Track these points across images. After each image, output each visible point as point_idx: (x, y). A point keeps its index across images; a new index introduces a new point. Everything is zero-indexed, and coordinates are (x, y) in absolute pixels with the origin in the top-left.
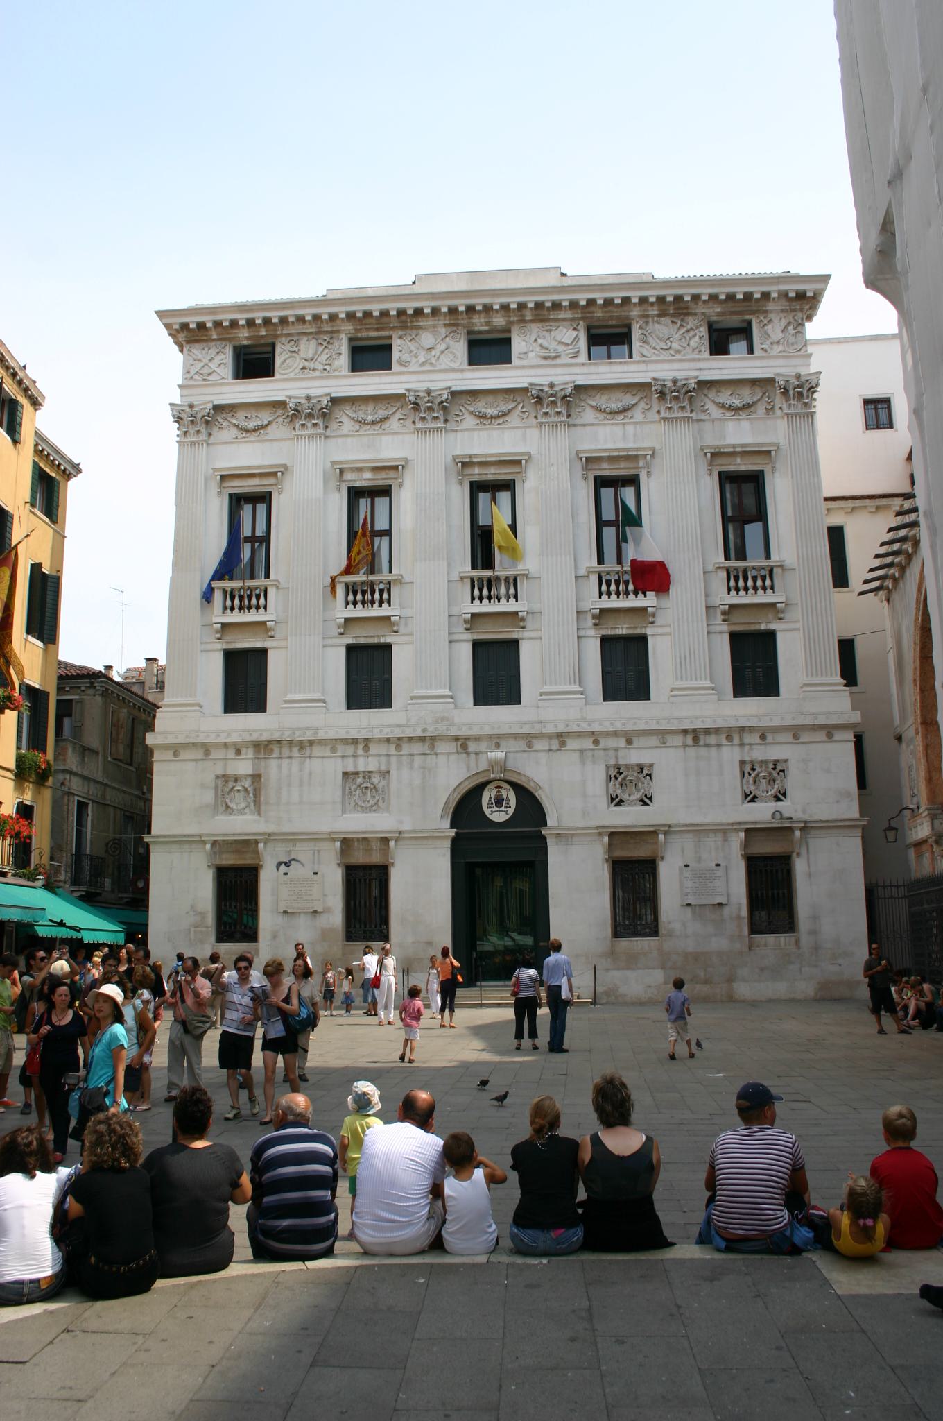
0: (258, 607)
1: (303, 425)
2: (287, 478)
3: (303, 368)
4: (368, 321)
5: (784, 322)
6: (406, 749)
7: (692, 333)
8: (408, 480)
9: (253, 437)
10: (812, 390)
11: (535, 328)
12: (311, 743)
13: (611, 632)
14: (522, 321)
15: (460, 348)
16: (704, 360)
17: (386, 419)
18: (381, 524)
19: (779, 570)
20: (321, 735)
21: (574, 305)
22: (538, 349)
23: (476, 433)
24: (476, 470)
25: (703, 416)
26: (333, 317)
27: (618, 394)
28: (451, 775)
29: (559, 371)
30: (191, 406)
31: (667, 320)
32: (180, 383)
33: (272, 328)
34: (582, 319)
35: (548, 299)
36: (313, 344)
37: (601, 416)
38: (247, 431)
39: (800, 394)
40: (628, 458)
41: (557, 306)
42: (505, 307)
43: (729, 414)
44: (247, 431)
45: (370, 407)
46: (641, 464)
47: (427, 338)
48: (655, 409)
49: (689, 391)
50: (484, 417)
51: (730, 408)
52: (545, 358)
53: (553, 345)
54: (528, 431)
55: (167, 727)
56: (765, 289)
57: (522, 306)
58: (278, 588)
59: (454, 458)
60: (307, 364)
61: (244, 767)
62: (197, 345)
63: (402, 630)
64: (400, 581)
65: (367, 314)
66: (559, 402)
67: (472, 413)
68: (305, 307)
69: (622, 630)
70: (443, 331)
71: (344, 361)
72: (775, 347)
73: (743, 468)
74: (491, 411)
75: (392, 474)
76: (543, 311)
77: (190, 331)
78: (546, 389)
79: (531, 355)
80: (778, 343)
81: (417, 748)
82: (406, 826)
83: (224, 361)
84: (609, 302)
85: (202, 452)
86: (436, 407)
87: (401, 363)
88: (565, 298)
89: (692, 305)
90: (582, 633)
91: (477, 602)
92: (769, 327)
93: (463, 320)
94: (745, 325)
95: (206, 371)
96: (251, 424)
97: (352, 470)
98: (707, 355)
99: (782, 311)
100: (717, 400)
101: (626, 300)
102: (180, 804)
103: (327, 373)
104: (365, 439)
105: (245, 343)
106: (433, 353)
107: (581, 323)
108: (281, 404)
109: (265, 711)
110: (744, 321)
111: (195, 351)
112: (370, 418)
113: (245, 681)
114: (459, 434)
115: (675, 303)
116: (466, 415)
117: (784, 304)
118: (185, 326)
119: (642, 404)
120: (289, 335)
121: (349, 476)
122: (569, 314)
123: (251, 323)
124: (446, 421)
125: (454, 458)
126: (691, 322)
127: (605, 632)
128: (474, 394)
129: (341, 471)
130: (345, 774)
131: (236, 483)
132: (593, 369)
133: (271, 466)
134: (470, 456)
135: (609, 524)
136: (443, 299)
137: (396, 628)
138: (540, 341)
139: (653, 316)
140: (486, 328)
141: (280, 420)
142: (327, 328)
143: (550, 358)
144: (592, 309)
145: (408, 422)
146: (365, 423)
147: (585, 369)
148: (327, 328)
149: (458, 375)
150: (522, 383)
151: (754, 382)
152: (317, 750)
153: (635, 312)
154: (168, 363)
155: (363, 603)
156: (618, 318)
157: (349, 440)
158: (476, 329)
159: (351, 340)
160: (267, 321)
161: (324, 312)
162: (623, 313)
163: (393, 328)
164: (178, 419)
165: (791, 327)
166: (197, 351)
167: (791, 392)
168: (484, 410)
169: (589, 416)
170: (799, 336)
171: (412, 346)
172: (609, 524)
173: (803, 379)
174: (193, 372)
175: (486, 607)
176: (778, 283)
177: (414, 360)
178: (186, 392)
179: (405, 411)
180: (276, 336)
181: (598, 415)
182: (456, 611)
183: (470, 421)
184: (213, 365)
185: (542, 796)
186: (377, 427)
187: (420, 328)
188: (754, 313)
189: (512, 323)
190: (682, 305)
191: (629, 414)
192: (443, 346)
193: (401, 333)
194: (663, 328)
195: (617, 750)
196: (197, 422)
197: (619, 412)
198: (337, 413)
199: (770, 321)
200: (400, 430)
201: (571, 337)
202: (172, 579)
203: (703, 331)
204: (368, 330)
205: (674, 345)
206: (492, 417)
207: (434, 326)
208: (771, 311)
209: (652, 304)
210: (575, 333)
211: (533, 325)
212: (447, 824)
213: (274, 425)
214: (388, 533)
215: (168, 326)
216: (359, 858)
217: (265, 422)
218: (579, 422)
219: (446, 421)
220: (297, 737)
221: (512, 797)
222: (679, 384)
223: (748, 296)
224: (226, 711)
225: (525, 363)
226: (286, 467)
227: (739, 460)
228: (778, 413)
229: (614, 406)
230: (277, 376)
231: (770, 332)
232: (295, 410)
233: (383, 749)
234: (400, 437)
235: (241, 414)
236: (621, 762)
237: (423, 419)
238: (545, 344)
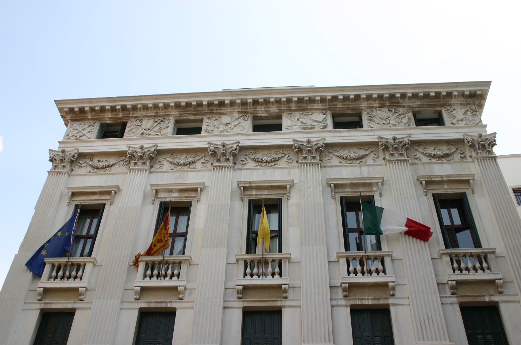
0: (76, 277)
1: (136, 163)
2: (118, 195)
3: (142, 134)
5: (463, 110)
7: (402, 116)
8: (204, 198)
10: (493, 144)
11: (297, 115)
13: (358, 302)
14: (290, 111)
15: (248, 124)
16: (413, 129)
17: (193, 162)
18: (181, 229)
19: (492, 255)
21: (323, 100)
22: (300, 124)
23: (255, 171)
24: (254, 192)
25: (416, 161)
26: (166, 106)
27: (355, 150)
29: (314, 135)
31: (386, 109)
32: (61, 139)
33: (126, 112)
34: (329, 109)
36: (151, 122)
37: (344, 162)
38: (97, 168)
39: (483, 146)
40: (364, 185)
41: (312, 101)
42: (278, 102)
43: (434, 160)
44: (97, 168)
45: (184, 156)
46: (374, 189)
47: (225, 119)
48: (382, 157)
49: (405, 145)
51: (434, 157)
52: (304, 129)
53: (310, 123)
54: (292, 170)
56: (449, 90)
57: (289, 101)
58: (95, 265)
59: (239, 183)
60: (145, 131)
62: (77, 123)
63: (186, 298)
64: (189, 262)
65: (188, 105)
66: (314, 152)
67: (253, 160)
68: (149, 99)
69: (368, 301)
70: (237, 116)
72: (460, 123)
73: (450, 191)
74: (265, 158)
75: (193, 194)
76: (302, 102)
77: (74, 113)
78: (304, 144)
79: (294, 127)
80: (462, 120)
84: (346, 98)
85: (64, 178)
86: (228, 154)
87: (207, 131)
89: (401, 101)
90: (334, 303)
91: (248, 277)
92: (454, 112)
93: (250, 109)
94: (436, 116)
95: (80, 134)
96: (101, 164)
98: (414, 126)
99: (461, 104)
100: (425, 152)
101: (358, 97)
104: (177, 174)
105: (109, 122)
106: (229, 126)
107: (328, 111)
110: (436, 112)
111: (75, 125)
112: (182, 162)
114: (243, 172)
115: (391, 99)
117: (462, 100)
118: (72, 110)
119: (372, 155)
120: (137, 117)
121: (161, 195)
122: (320, 106)
123: (113, 109)
124: (235, 164)
125: (239, 183)
126: (401, 110)
127: (353, 302)
128: (255, 149)
129: (157, 192)
132: (337, 134)
133: (108, 187)
134: (250, 183)
135: (352, 230)
136: (238, 95)
137: (181, 296)
138: (300, 120)
139: (375, 107)
140: (266, 115)
141: (122, 163)
142: (162, 113)
143: (306, 129)
144: (335, 103)
146: (178, 164)
147: (332, 134)
148: (162, 113)
149: (246, 138)
150: (290, 142)
151: (449, 142)
153: (364, 105)
154: (55, 132)
155: (158, 276)
156: (353, 108)
157: (166, 174)
158: (259, 115)
159: (177, 122)
160: (124, 108)
162: (356, 105)
164: (52, 160)
165: (469, 113)
166: (76, 125)
167: (477, 146)
168: (261, 157)
169: (335, 161)
170: (475, 117)
171: (216, 123)
172: (352, 230)
173: (483, 138)
174: (70, 135)
175: (256, 281)
176: (457, 87)
177: (216, 130)
178: (62, 146)
179: (207, 158)
180: (129, 118)
181: (342, 161)
182: (231, 284)
183: (251, 164)
184: (84, 132)
187: (222, 114)
188: (443, 106)
189: (282, 111)
190: (394, 101)
191: (364, 160)
192: (236, 122)
193: (209, 116)
194: (384, 113)
197: (356, 159)
198: (160, 159)
199: (454, 109)
200: (203, 169)
201: (321, 118)
202: (16, 256)
203: (410, 115)
205: (391, 122)
206: (267, 162)
208: (454, 105)
209: (375, 99)
210: (324, 116)
211: (296, 113)
213: (117, 166)
214: (184, 235)
215: (60, 110)
217: (111, 163)
218: (328, 164)
219: (235, 164)
222: (397, 141)
223: (438, 95)
225: (291, 131)
226: (118, 187)
227: (446, 187)
228: (470, 159)
229: (352, 155)
230: (125, 137)
231: (455, 115)
232: (131, 154)
234: (202, 173)
238: (304, 121)
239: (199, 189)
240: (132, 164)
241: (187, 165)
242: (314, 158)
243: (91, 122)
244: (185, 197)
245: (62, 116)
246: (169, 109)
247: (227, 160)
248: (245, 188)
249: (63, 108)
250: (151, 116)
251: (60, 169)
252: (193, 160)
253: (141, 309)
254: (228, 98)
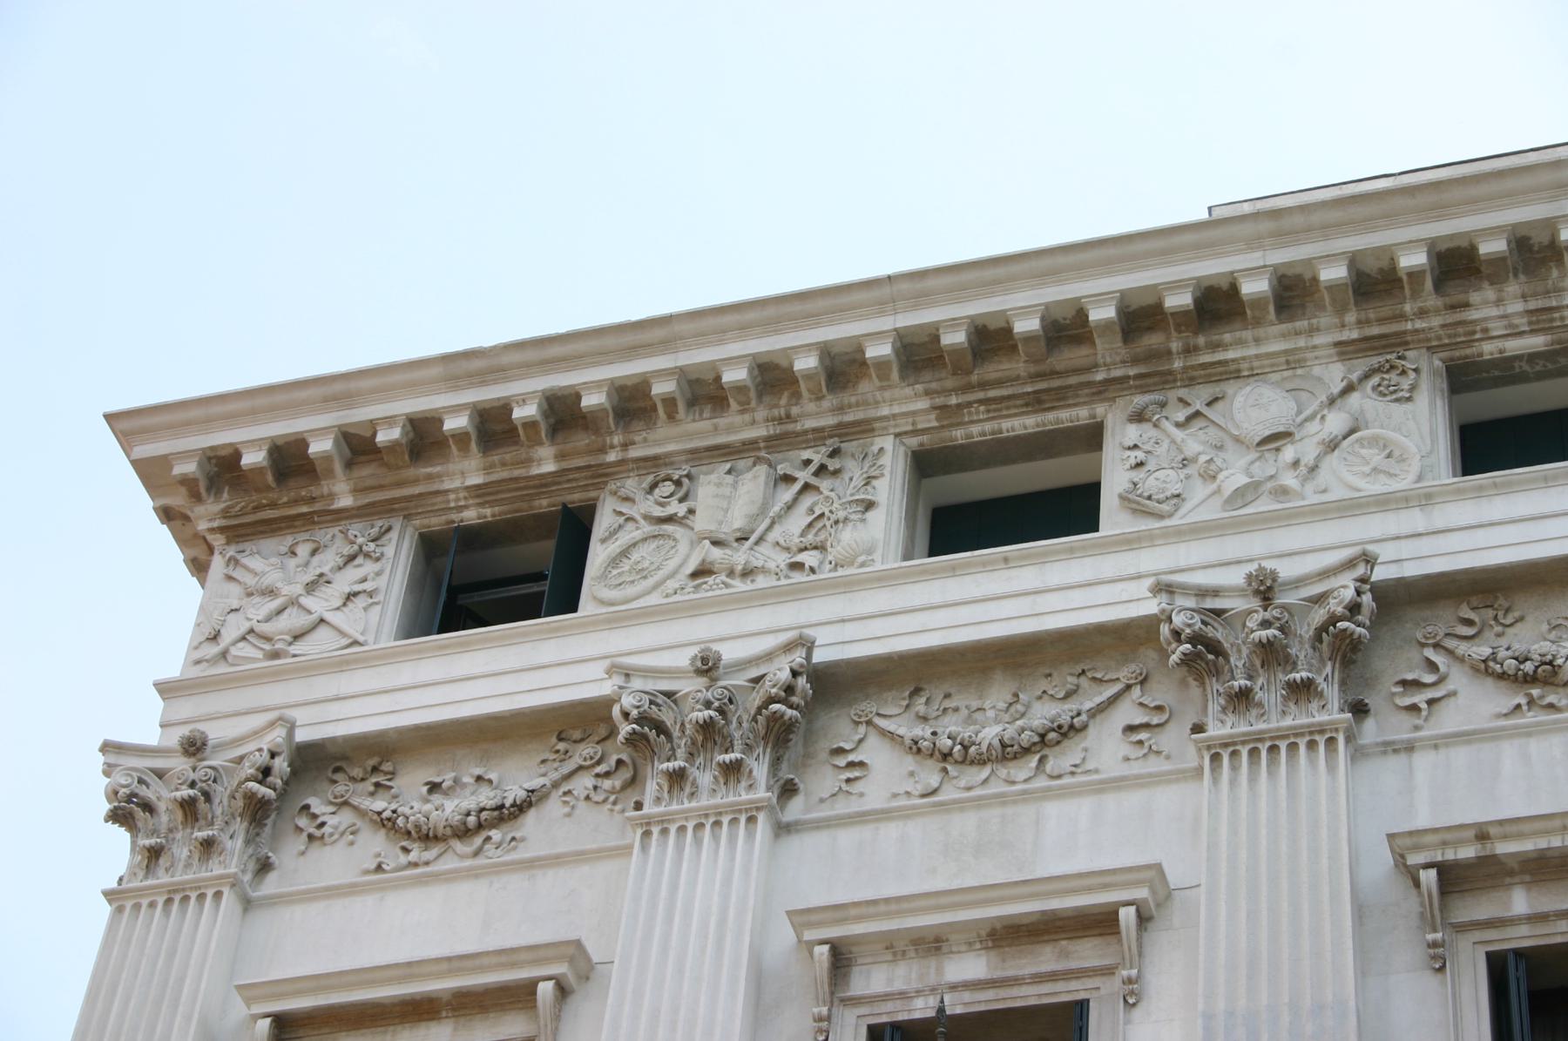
2: (581, 1008)
3: (701, 572)
4: (993, 369)
9: (456, 857)
15: (1420, 425)
17: (1068, 731)
23: (1509, 751)
24: (1520, 902)
26: (842, 368)
32: (173, 669)
33: (582, 440)
36: (753, 483)
38: (428, 837)
44: (428, 837)
45: (997, 696)
47: (1255, 407)
60: (717, 553)
62: (271, 544)
65: (991, 339)
67: (1486, 669)
70: (1335, 374)
75: (1088, 953)
77: (240, 487)
85: (214, 924)
86: (1299, 650)
87: (1136, 504)
93: (1424, 314)
95: (292, 620)
96: (450, 809)
97: (897, 947)
104: (965, 824)
105: (471, 516)
106: (1289, 453)
111: (255, 563)
112: (990, 734)
114: (1423, 761)
116: (1458, 679)
118: (223, 469)
120: (654, 461)
121: (872, 979)
123: (494, 428)
124: (1360, 710)
129: (841, 959)
133: (508, 956)
134: (1482, 834)
136: (1327, 230)
140: (1537, 342)
141: (584, 782)
142: (815, 415)
146: (963, 755)
148: (815, 415)
149: (1414, 520)
154: (131, 619)
158: (1489, 349)
159: (925, 464)
160: (563, 414)
161: (801, 348)
163: (1106, 390)
164: (127, 811)
166: (264, 562)
171: (1193, 442)
174: (228, 635)
177: (1200, 491)
178: (186, 708)
179: (1161, 692)
180: (601, 475)
183: (1473, 703)
184: (317, 605)
186: (1023, 770)
187: (1231, 373)
192: (1336, 422)
193: (1140, 400)
198: (840, 729)
200: (1136, 768)
204: (996, 406)
207: (1292, 361)
215: (151, 473)
219: (1360, 710)
226: (575, 951)
230: (586, 606)
232: (642, 719)
234: (1133, 799)
235: (410, 784)
237: (1241, 699)
239: (1127, 916)
240: (652, 787)
241: (1027, 751)
243: (355, 529)
244: (1039, 978)
245: (167, 515)
246: (866, 387)
247: (1302, 691)
248: (1453, 879)
249: (165, 461)
250: (749, 447)
251: (181, 867)
252: (1062, 712)
254: (1254, 259)
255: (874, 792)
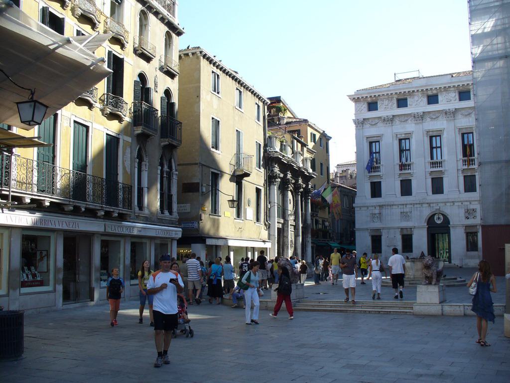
6: (416, 206)
8: (414, 136)
9: (374, 126)
12: (393, 205)
14: (441, 91)
15: (425, 100)
20: (395, 203)
21: (454, 86)
28: (427, 212)
30: (358, 120)
35: (447, 86)
37: (463, 116)
41: (449, 87)
44: (372, 125)
47: (416, 98)
50: (432, 118)
52: (448, 101)
55: (358, 201)
61: (377, 211)
64: (413, 163)
71: (395, 105)
75: (409, 135)
77: (356, 99)
81: (418, 206)
82: (416, 225)
83: (365, 106)
84: (463, 85)
88: (451, 85)
102: (362, 220)
103: (391, 109)
108: (380, 117)
109: (381, 197)
113: (376, 190)
118: (354, 98)
122: (453, 89)
129: (397, 135)
130: (401, 212)
131: (370, 139)
142: (390, 96)
143: (449, 101)
145: (413, 121)
146: (402, 121)
148: (390, 96)
152: (394, 207)
153: (471, 87)
155: (404, 169)
164: (355, 124)
169: (460, 116)
175: (434, 169)
182: (427, 170)
183: (429, 120)
184: (362, 108)
185: (450, 218)
195: (467, 205)
196: (360, 123)
198: (395, 119)
201: (454, 95)
212: (426, 224)
214: (409, 150)
215: (350, 98)
216: (405, 232)
220: (389, 203)
221: (442, 217)
224: (372, 197)
233: (410, 206)
236: (468, 208)
242: (452, 117)
253: (401, 180)
255: (397, 124)
